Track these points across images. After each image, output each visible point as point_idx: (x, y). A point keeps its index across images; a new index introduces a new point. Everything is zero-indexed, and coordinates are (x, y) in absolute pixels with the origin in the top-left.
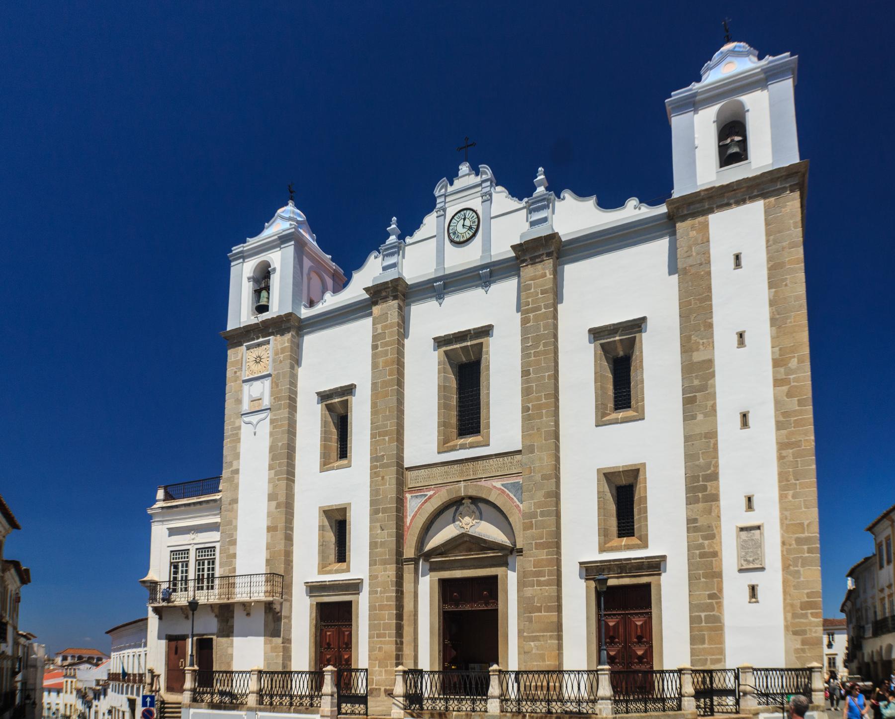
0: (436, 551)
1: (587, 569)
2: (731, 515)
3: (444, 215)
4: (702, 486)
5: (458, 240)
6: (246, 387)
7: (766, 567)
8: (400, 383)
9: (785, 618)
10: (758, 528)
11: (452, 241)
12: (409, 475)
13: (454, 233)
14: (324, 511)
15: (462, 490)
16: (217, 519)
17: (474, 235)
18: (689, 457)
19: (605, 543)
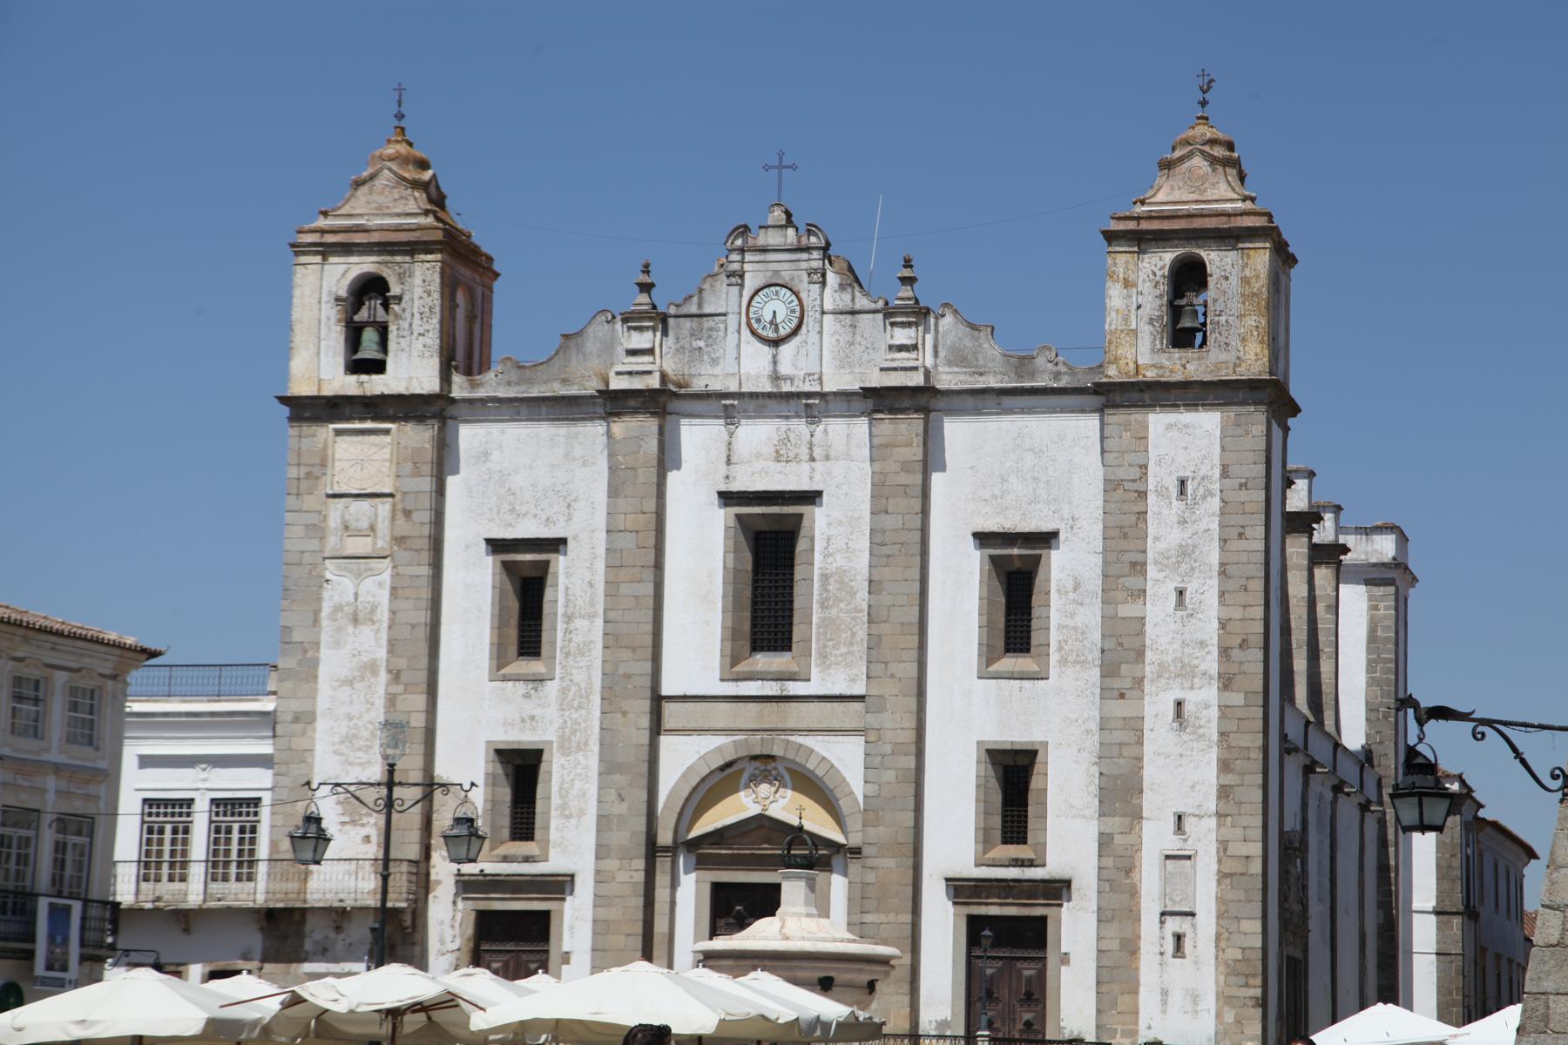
0: (718, 836)
1: (956, 888)
2: (1156, 837)
3: (742, 286)
4: (1120, 793)
5: (764, 333)
6: (336, 509)
7: (1197, 911)
8: (659, 566)
9: (1217, 981)
10: (1189, 857)
11: (754, 333)
12: (668, 708)
13: (758, 320)
14: (499, 752)
15: (757, 745)
16: (265, 748)
17: (795, 332)
18: (1106, 753)
19: (985, 853)
